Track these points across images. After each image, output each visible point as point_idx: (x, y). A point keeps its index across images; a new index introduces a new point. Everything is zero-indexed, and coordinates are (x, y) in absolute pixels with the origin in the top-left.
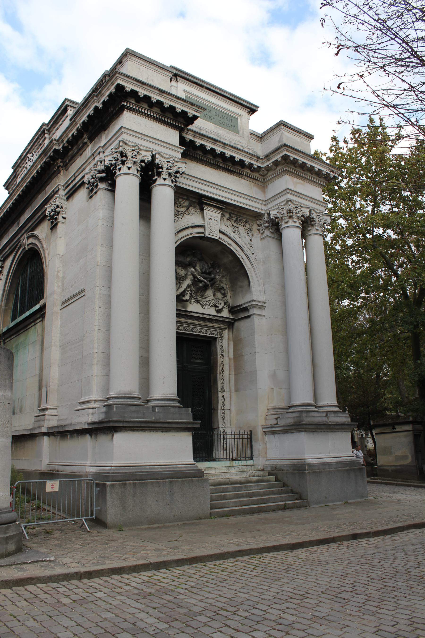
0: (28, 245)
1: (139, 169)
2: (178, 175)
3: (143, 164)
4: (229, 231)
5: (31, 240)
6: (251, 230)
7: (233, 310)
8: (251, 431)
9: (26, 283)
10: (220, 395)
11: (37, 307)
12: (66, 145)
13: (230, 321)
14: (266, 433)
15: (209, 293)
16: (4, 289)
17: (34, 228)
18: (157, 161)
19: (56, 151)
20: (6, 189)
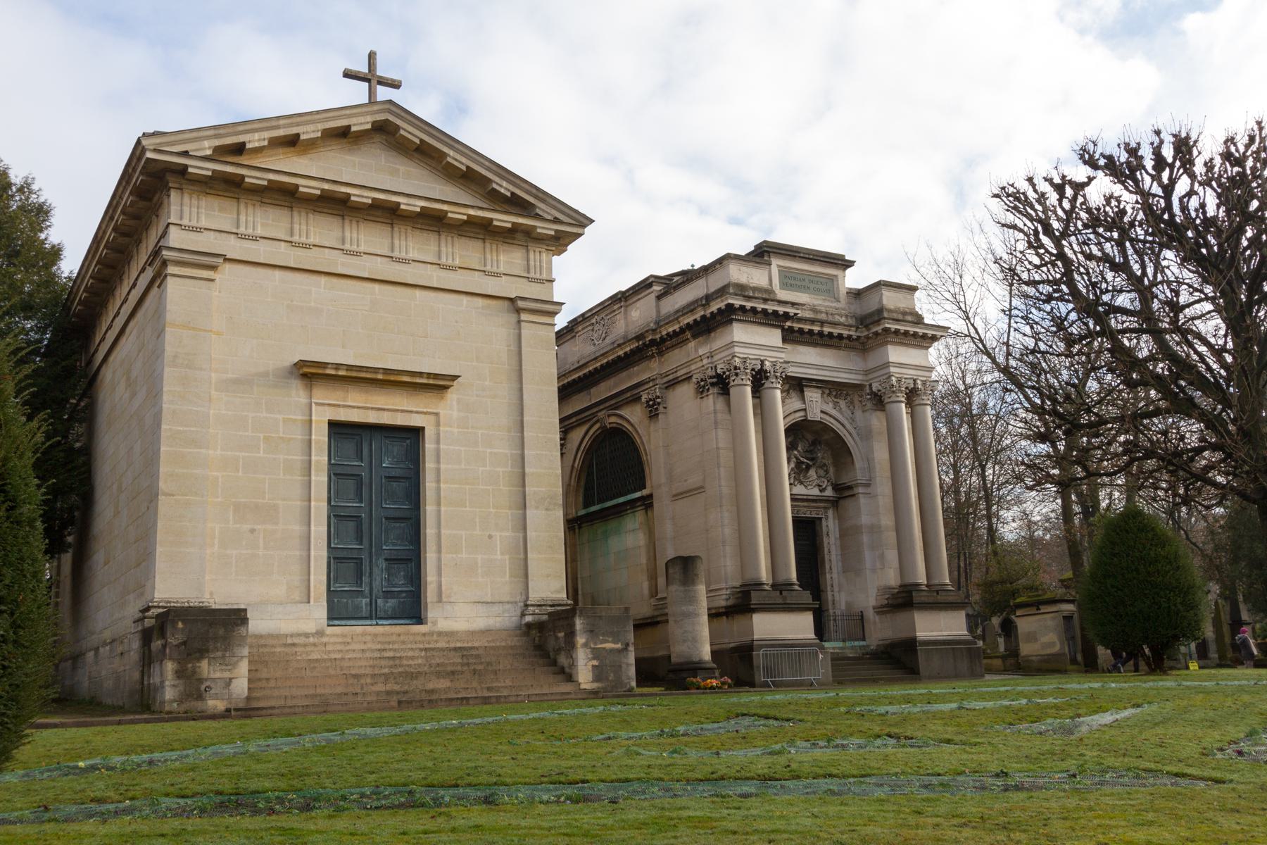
4: (829, 408)
5: (613, 419)
6: (852, 402)
7: (837, 488)
10: (828, 576)
11: (638, 495)
15: (812, 472)
19: (653, 342)
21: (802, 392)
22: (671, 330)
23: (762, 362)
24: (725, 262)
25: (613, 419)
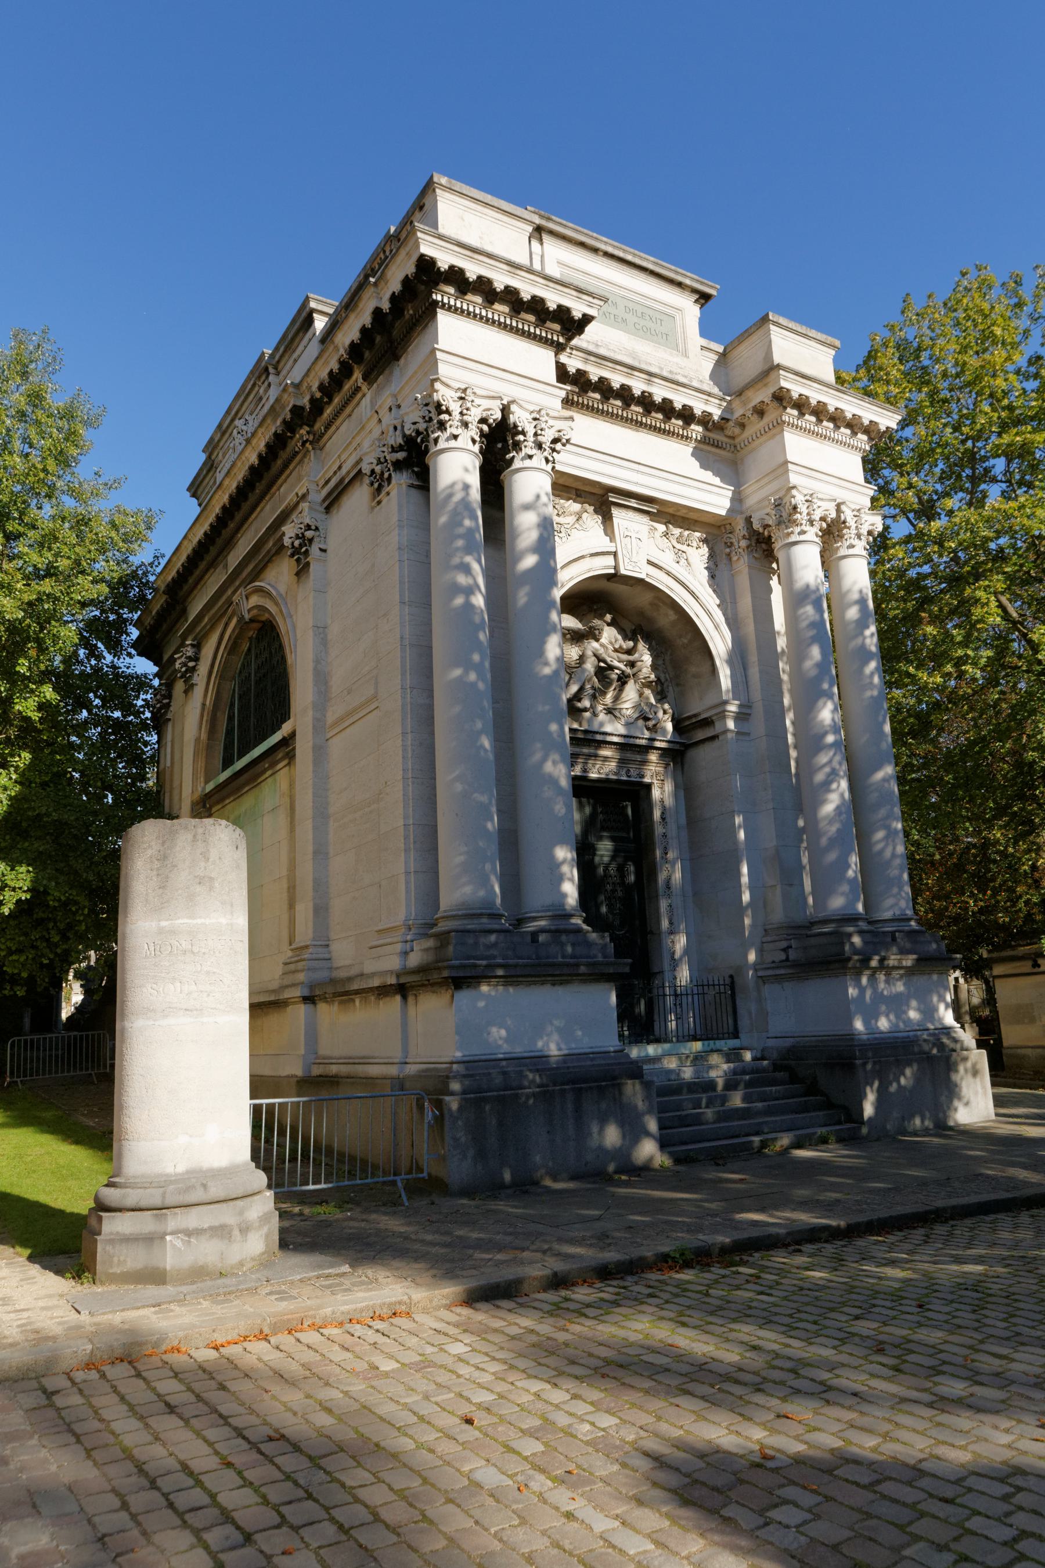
0: (249, 611)
1: (477, 439)
2: (558, 446)
3: (485, 428)
5: (254, 600)
8: (731, 977)
9: (249, 689)
12: (318, 395)
13: (677, 747)
14: (763, 980)
16: (204, 705)
17: (257, 574)
18: (512, 419)
19: (297, 410)
20: (194, 495)
21: (607, 519)
22: (324, 374)
23: (505, 410)
24: (427, 201)
25: (254, 600)
